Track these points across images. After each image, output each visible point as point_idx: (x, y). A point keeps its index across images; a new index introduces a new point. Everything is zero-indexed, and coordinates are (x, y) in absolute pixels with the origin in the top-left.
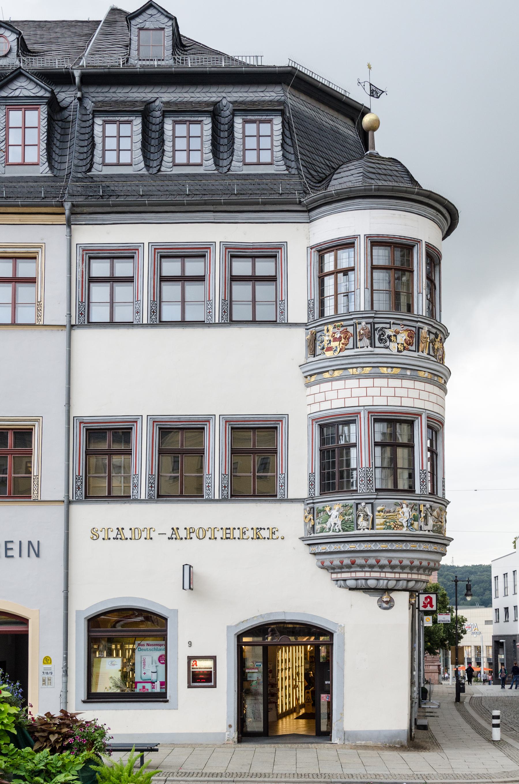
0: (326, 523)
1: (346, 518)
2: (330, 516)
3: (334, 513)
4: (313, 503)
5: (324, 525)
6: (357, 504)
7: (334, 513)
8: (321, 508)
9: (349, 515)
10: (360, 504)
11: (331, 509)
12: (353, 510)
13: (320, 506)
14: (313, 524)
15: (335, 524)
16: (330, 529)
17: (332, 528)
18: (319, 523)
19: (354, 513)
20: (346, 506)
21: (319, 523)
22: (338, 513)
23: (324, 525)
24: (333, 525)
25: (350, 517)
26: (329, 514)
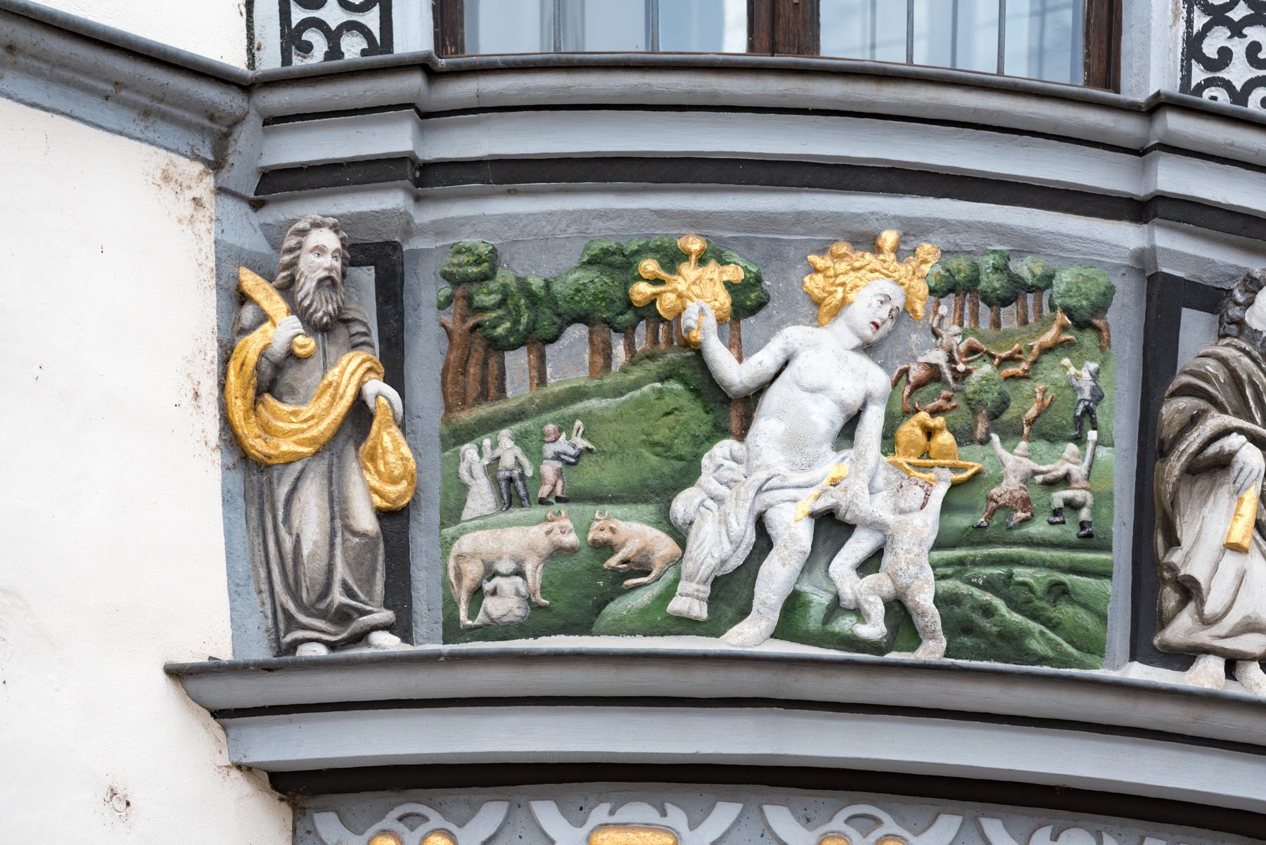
0: (657, 494)
1: (1013, 463)
2: (734, 410)
3: (820, 368)
4: (427, 177)
5: (635, 532)
6: (1166, 298)
7: (820, 368)
8: (556, 268)
9: (1047, 432)
10: (1211, 298)
11: (747, 303)
12: (1103, 374)
13: (543, 235)
14: (397, 492)
15: (831, 526)
16: (731, 593)
17: (775, 580)
18: (513, 492)
19: (1120, 417)
20: (1015, 291)
21: (513, 492)
22: (877, 379)
23: (635, 532)
24: (794, 531)
25: (1066, 459)
26: (734, 371)
